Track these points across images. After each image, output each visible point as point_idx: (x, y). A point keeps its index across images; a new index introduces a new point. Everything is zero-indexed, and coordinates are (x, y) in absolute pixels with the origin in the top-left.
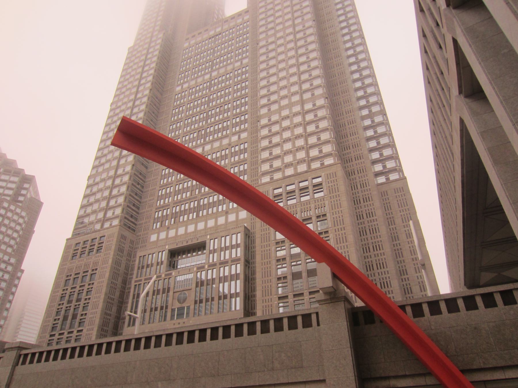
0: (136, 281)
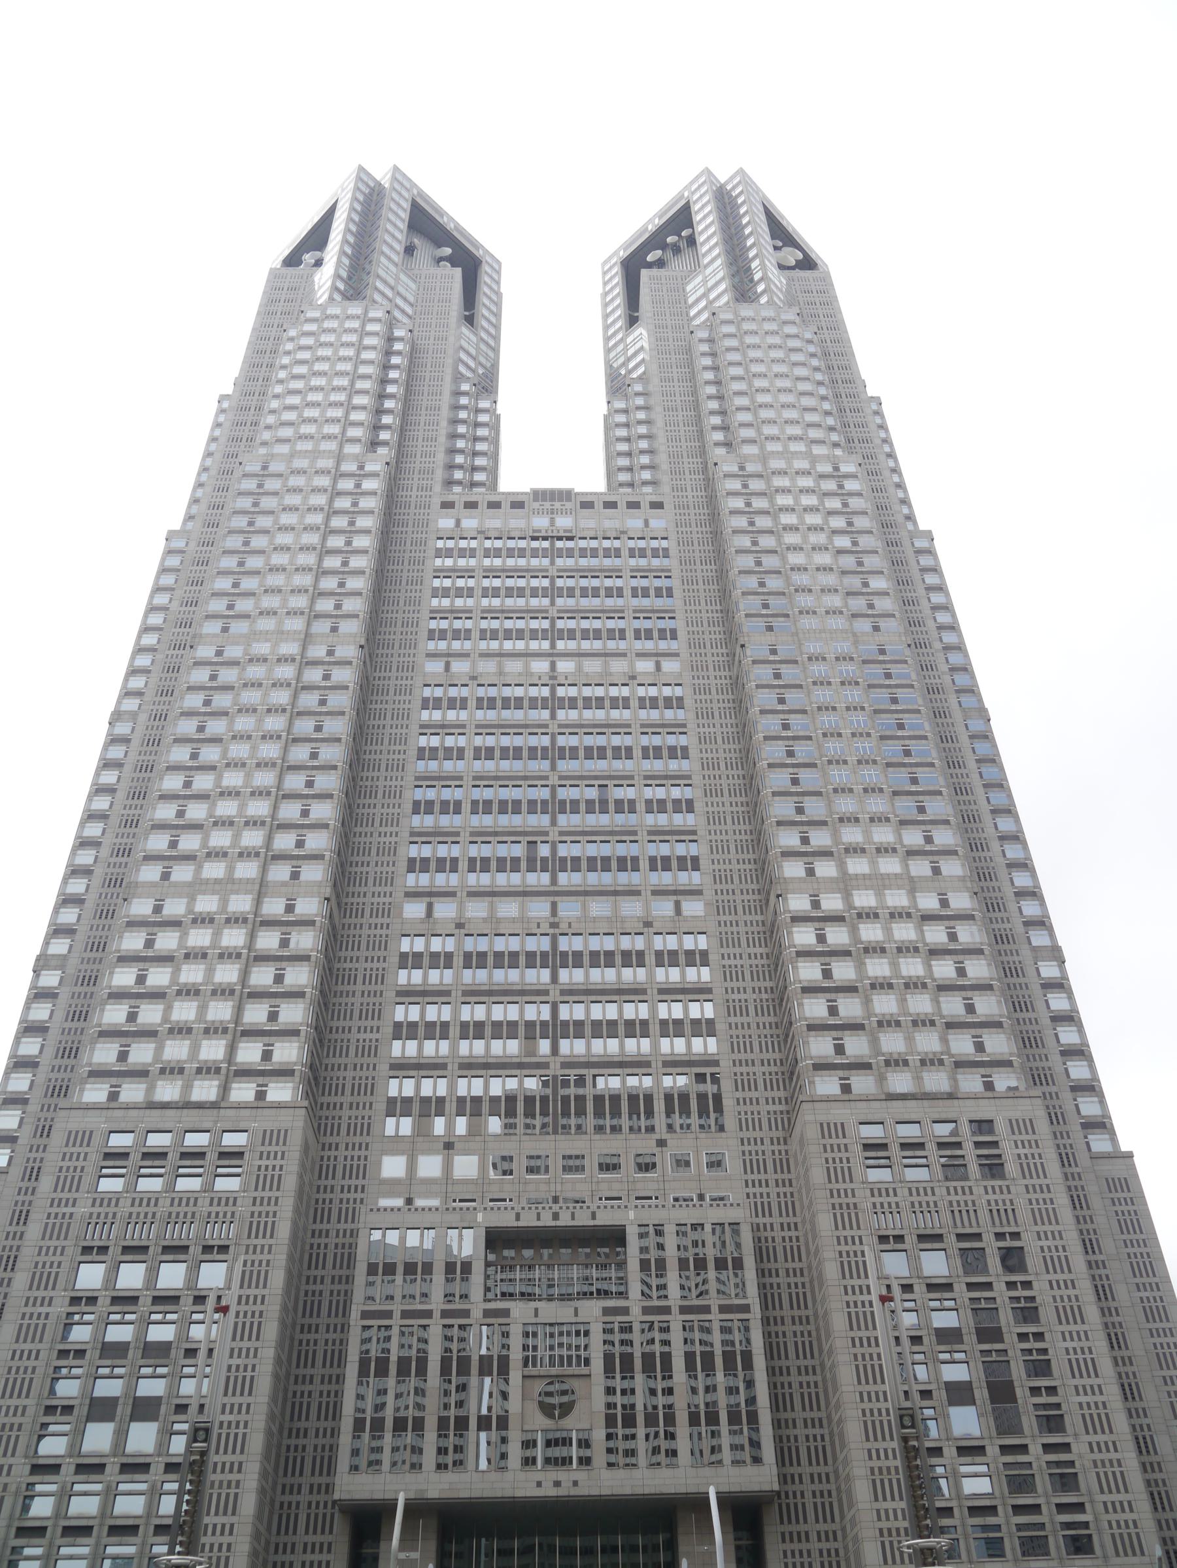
0: (365, 1315)
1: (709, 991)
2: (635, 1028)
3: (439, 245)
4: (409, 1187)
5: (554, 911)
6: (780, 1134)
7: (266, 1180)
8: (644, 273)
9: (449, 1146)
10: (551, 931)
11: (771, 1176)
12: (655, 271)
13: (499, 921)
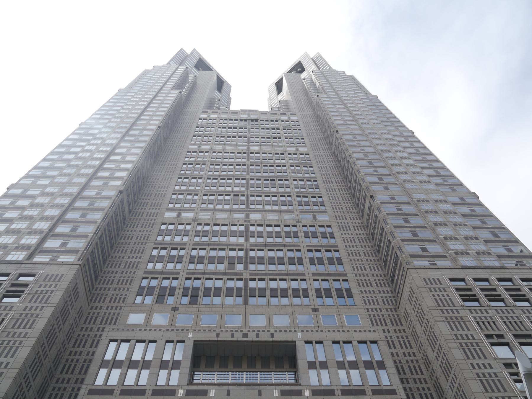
9: (175, 309)
10: (246, 223)
13: (216, 219)
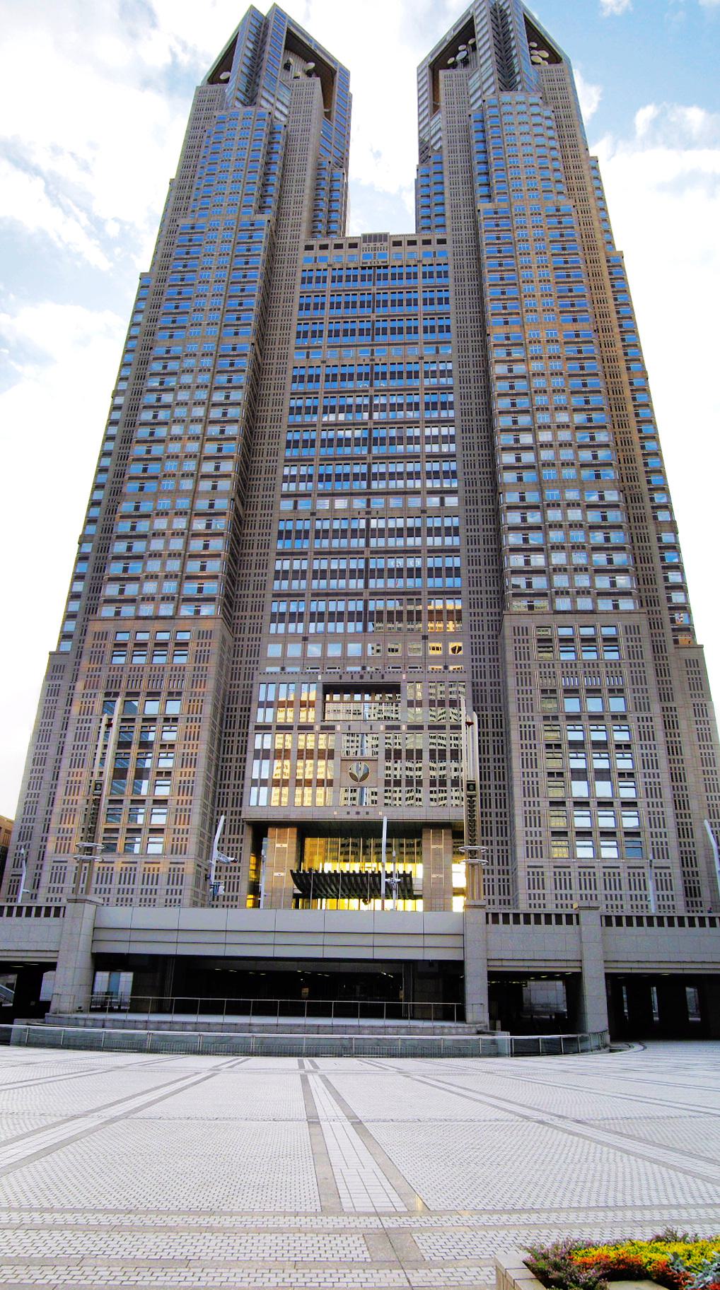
1: (458, 551)
2: (414, 573)
3: (308, 61)
4: (283, 662)
5: (368, 505)
6: (494, 633)
7: (201, 657)
8: (442, 73)
9: (305, 639)
11: (487, 656)
12: (448, 72)
13: (336, 511)
